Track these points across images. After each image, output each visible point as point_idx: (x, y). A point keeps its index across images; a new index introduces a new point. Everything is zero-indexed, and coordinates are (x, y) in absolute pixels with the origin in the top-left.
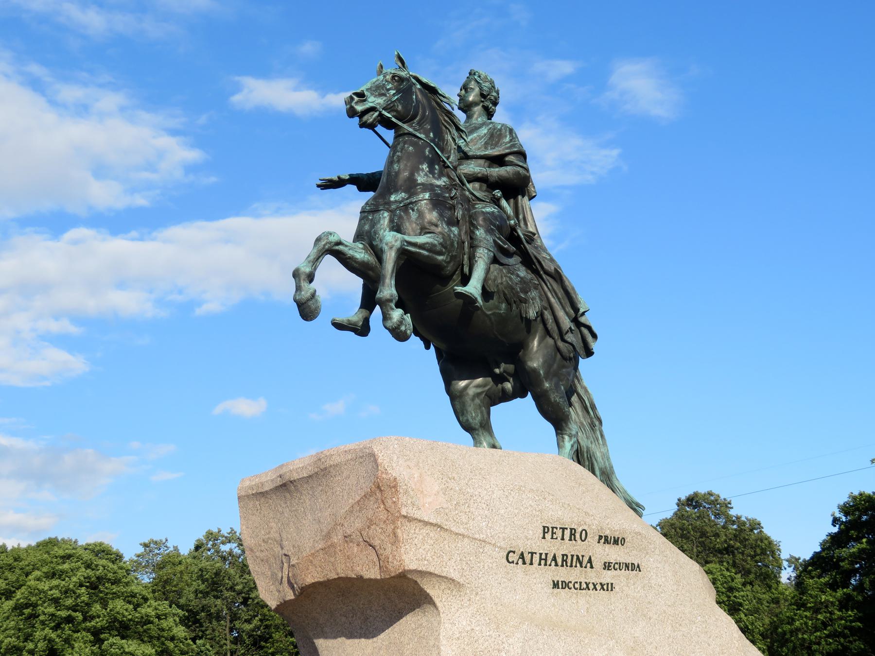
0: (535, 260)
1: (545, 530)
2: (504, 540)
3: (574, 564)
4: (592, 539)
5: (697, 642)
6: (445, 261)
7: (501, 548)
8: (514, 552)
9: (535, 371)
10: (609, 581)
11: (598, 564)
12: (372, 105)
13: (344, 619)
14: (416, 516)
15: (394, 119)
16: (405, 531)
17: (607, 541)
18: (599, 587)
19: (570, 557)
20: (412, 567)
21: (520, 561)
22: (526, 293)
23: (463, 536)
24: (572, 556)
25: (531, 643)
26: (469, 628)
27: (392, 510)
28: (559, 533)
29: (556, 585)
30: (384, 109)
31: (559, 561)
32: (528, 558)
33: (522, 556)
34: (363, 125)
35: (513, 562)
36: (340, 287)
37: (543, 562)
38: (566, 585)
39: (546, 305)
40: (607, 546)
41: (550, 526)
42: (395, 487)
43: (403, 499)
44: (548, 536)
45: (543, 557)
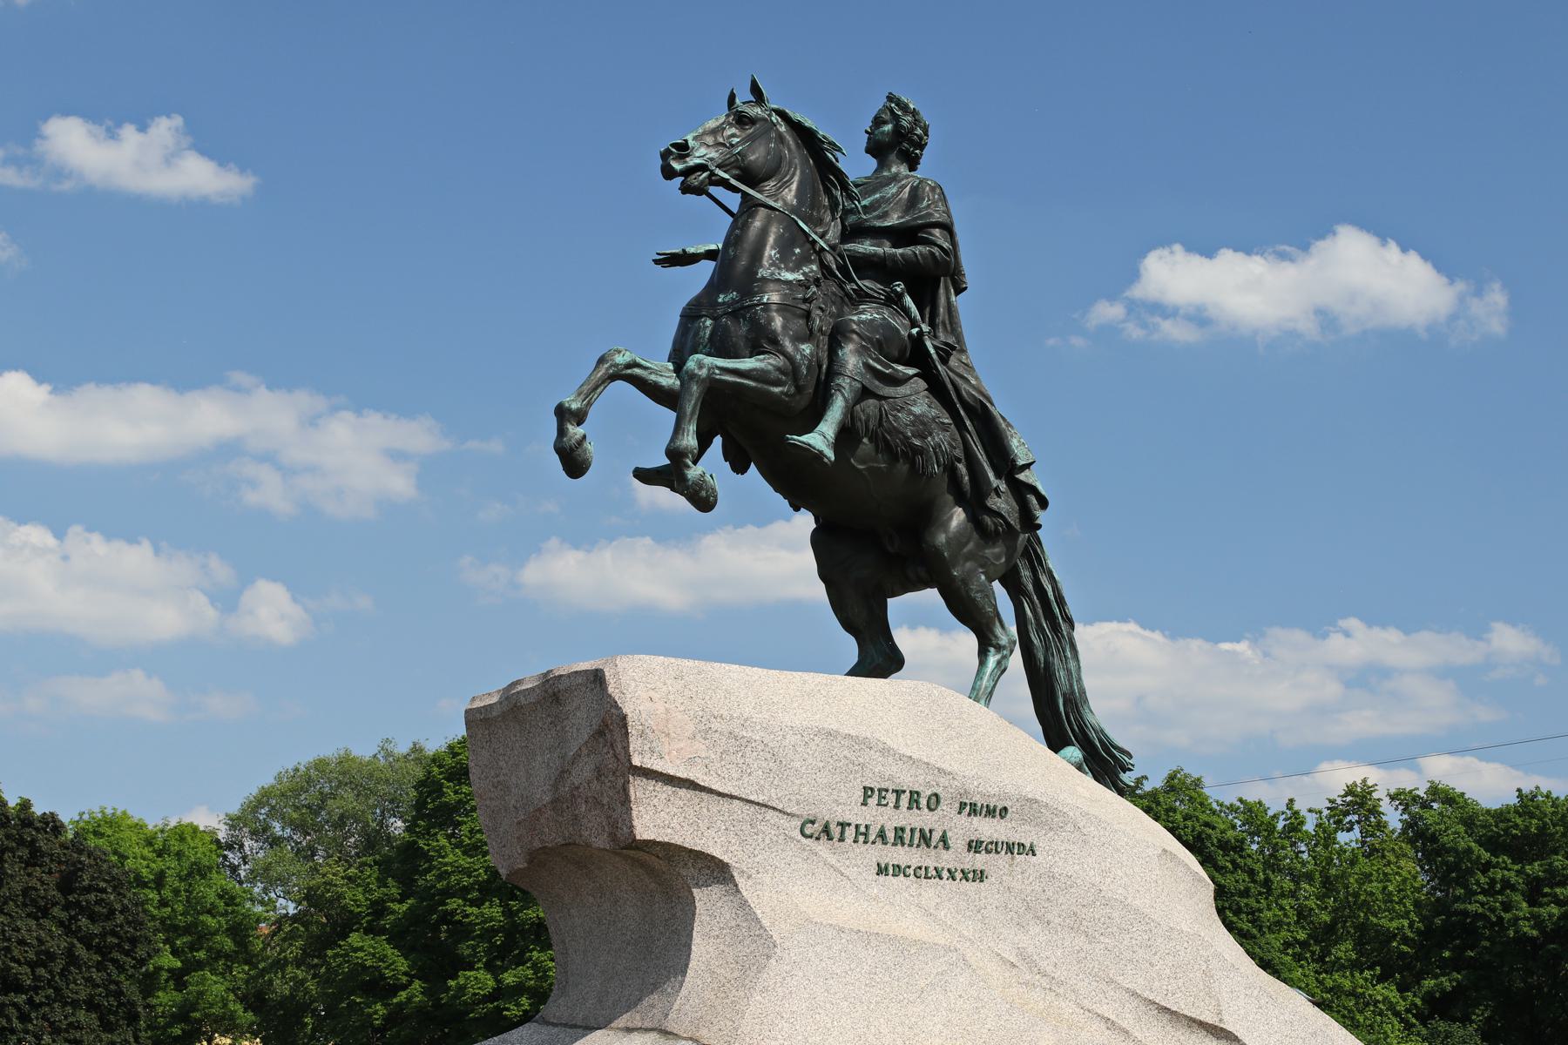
0: (950, 386)
1: (868, 791)
2: (798, 803)
3: (916, 841)
4: (947, 808)
5: (1131, 961)
6: (786, 394)
7: (793, 815)
8: (813, 822)
9: (937, 552)
10: (979, 867)
11: (958, 842)
12: (698, 161)
13: (591, 899)
14: (655, 768)
15: (733, 182)
16: (639, 789)
17: (974, 810)
18: (958, 875)
19: (908, 831)
20: (646, 836)
21: (824, 837)
22: (923, 437)
23: (732, 797)
24: (912, 830)
25: (818, 948)
26: (733, 923)
27: (622, 757)
28: (891, 797)
29: (882, 870)
30: (719, 166)
31: (891, 835)
32: (836, 831)
33: (826, 830)
34: (686, 189)
35: (811, 837)
36: (635, 430)
37: (861, 838)
38: (898, 870)
39: (959, 453)
40: (976, 820)
41: (876, 786)
42: (625, 726)
43: (635, 744)
44: (873, 801)
45: (862, 829)
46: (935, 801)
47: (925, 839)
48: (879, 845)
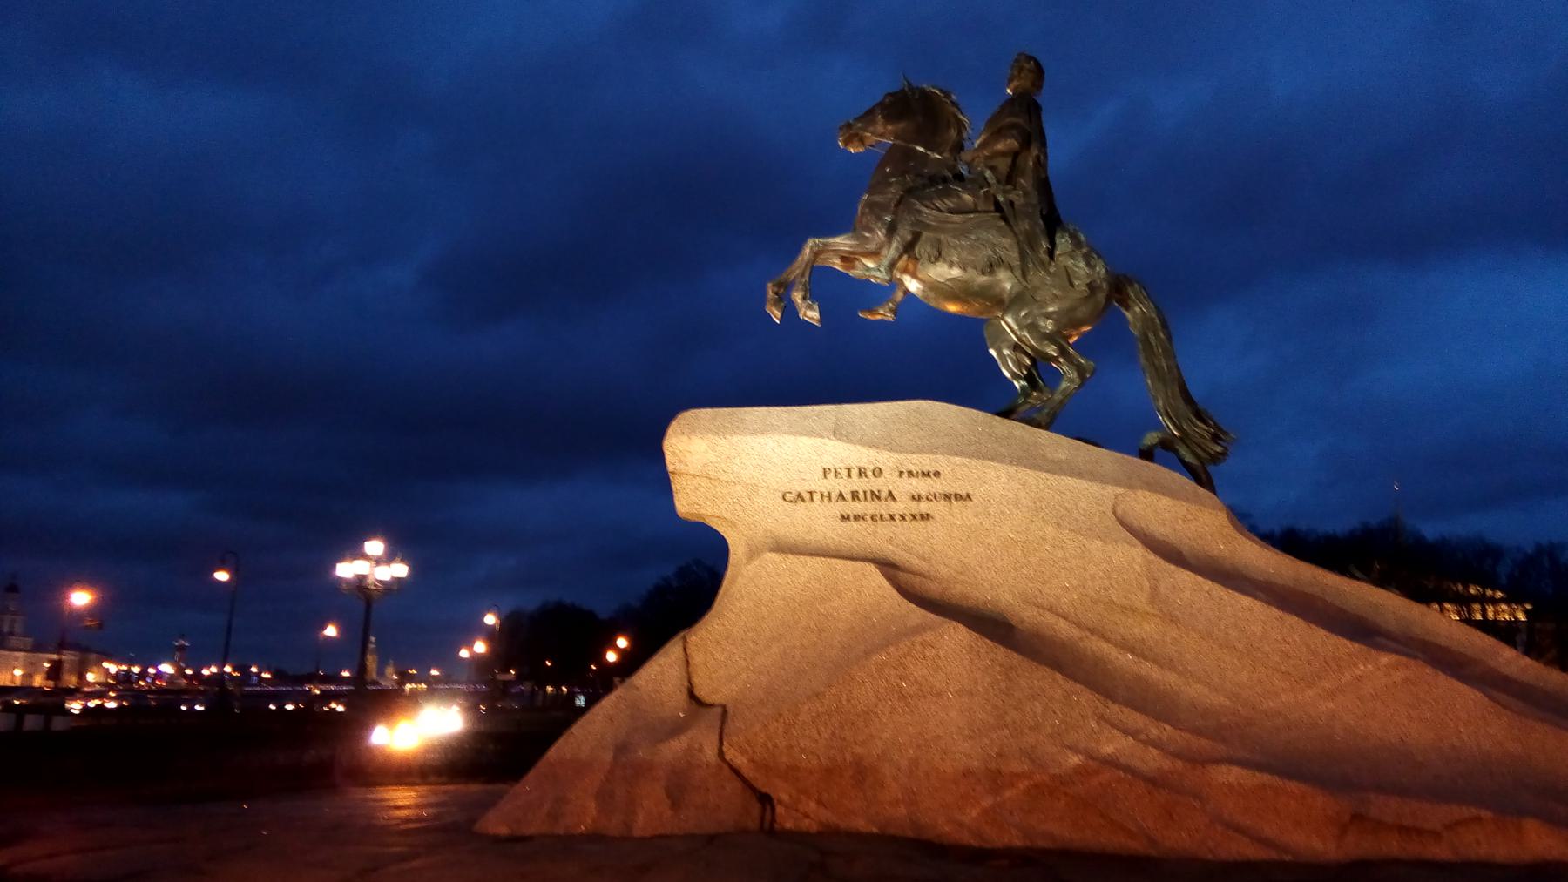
10: (924, 511)
28: (845, 472)
29: (845, 518)
32: (807, 496)
33: (799, 495)
40: (913, 480)
44: (831, 476)
46: (878, 472)
47: (876, 496)
48: (841, 503)
